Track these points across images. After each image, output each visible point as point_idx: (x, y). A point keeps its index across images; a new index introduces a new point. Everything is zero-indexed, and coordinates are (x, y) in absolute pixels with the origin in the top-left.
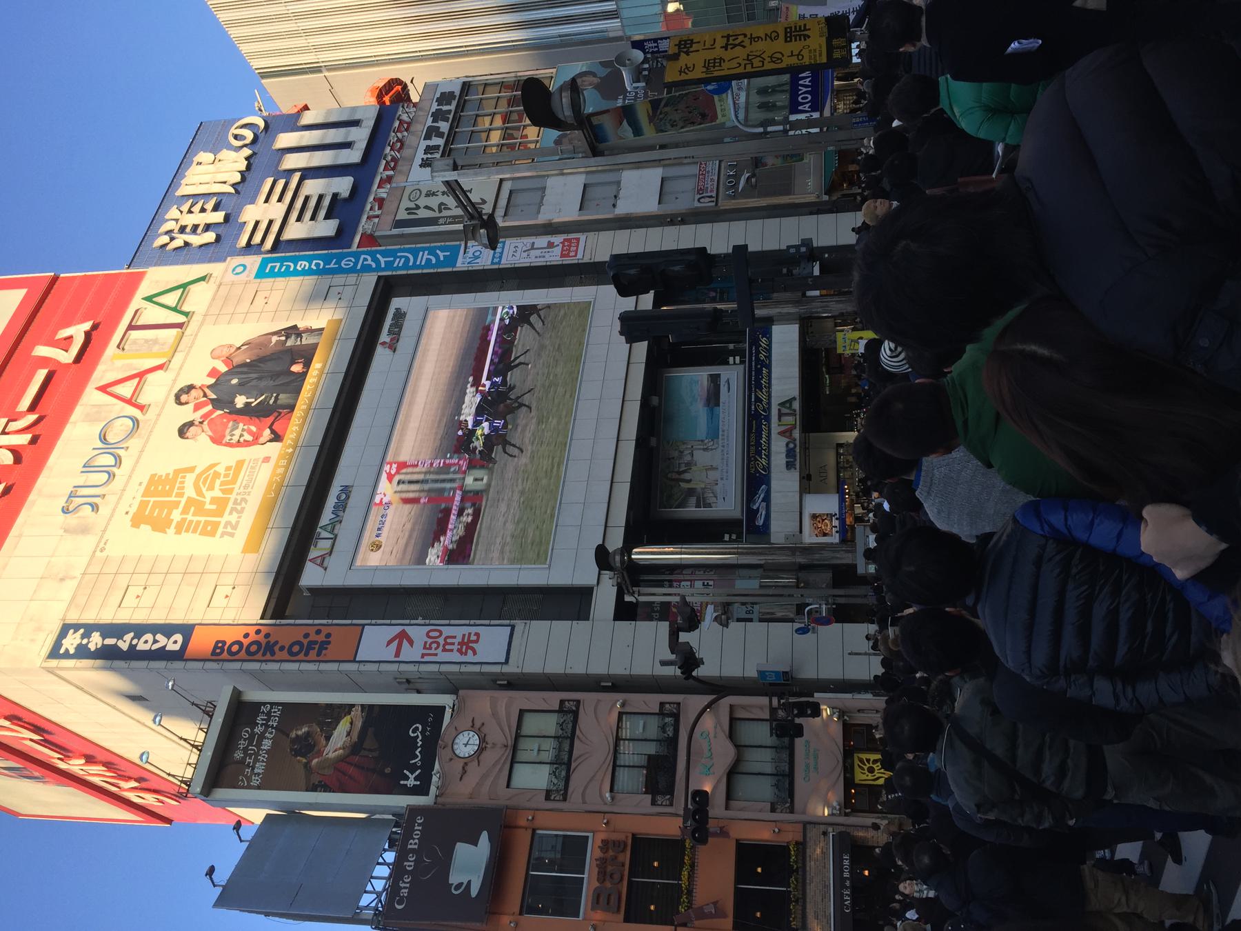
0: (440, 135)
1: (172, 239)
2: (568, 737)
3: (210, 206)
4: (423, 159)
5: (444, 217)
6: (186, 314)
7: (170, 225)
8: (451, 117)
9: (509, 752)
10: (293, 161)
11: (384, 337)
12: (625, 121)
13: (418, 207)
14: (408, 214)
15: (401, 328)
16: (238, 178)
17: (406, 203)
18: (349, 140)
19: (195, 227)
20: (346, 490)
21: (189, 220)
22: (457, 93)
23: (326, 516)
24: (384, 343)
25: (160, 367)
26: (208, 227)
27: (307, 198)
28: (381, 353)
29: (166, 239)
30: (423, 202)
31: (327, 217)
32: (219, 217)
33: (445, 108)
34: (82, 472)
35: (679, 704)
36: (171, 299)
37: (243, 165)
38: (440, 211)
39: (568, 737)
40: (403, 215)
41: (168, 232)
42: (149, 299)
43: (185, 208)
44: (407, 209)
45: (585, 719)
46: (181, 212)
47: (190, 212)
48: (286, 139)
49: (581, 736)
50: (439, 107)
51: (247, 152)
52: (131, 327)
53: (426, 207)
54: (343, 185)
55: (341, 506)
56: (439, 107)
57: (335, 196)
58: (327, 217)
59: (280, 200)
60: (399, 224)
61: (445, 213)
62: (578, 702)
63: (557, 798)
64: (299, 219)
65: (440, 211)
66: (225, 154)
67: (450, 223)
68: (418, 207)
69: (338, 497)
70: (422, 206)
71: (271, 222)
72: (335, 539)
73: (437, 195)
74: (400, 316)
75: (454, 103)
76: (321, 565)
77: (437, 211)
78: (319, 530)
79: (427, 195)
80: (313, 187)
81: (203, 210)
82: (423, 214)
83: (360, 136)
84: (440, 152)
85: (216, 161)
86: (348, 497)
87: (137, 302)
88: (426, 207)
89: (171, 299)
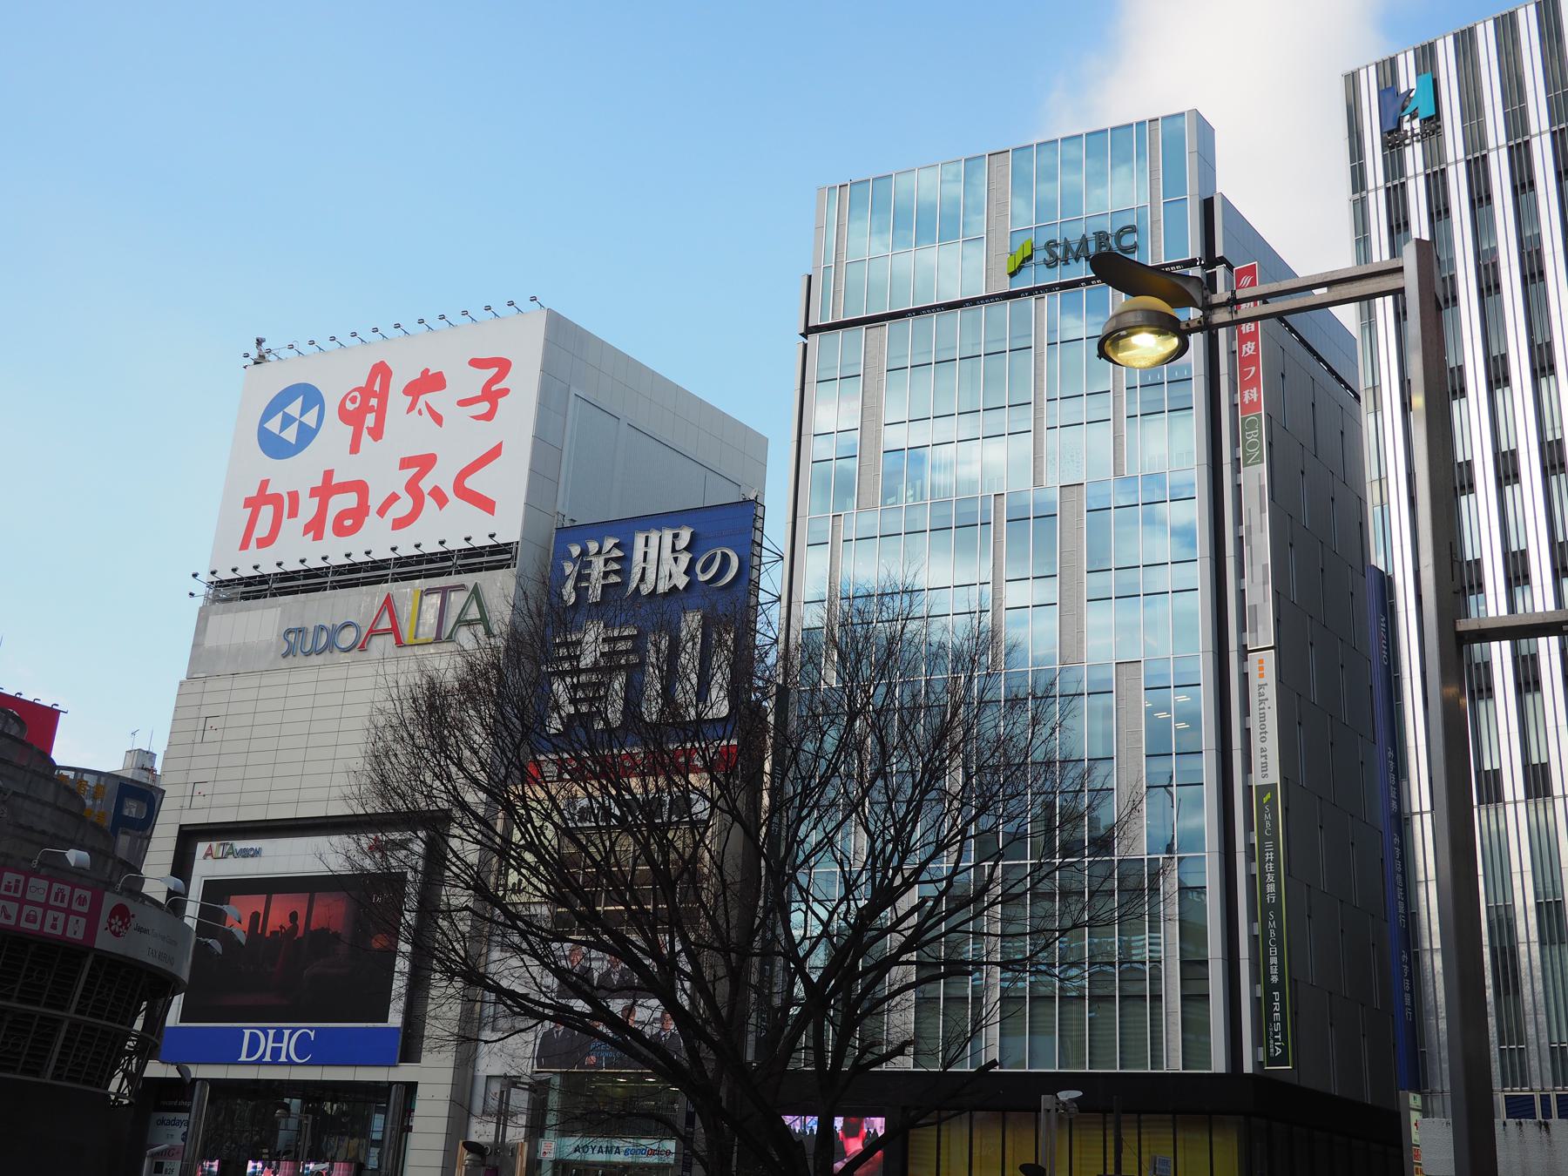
1: (574, 561)
3: (614, 579)
7: (593, 547)
16: (646, 589)
20: (257, 853)
21: (598, 566)
23: (240, 845)
25: (399, 643)
26: (581, 592)
32: (595, 594)
41: (584, 552)
42: (476, 593)
43: (617, 553)
47: (606, 562)
55: (245, 854)
66: (685, 559)
76: (207, 855)
78: (230, 842)
81: (606, 575)
86: (252, 856)
87: (469, 579)
89: (473, 613)
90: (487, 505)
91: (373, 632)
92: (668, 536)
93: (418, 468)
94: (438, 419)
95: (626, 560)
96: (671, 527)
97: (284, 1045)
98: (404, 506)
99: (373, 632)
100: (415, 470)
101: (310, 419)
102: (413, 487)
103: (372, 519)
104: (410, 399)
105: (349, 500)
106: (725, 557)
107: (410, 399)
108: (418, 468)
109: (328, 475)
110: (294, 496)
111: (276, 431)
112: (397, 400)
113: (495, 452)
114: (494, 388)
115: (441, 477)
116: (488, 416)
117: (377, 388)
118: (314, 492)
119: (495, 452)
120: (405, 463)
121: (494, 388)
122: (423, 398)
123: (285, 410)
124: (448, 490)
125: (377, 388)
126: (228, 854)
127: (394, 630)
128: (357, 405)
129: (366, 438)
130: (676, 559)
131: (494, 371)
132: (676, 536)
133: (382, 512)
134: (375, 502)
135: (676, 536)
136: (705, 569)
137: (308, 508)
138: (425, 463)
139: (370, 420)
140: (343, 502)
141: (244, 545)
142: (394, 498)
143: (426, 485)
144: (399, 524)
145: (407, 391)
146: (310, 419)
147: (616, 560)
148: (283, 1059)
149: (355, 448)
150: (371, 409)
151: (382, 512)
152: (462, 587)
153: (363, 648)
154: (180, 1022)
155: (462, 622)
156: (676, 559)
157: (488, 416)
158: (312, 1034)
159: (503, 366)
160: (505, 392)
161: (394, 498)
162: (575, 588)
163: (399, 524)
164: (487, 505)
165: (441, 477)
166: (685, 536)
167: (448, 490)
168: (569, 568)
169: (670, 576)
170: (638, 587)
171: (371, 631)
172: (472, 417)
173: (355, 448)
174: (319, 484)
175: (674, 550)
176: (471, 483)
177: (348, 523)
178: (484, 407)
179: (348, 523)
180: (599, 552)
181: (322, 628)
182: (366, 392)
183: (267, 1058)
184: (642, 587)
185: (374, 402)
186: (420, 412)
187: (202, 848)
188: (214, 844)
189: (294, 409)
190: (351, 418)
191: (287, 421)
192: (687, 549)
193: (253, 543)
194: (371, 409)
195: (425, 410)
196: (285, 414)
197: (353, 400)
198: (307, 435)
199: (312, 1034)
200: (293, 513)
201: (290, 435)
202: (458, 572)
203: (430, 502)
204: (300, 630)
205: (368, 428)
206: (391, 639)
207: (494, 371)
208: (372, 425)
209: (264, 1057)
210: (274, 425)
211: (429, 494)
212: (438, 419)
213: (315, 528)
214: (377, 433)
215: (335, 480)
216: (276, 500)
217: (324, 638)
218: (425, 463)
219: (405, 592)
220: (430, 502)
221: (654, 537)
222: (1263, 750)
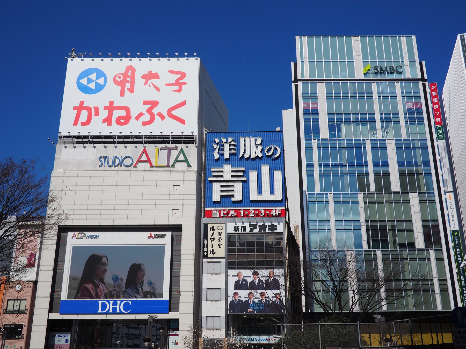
0: (251, 230)
1: (217, 144)
2: (19, 312)
3: (233, 151)
4: (239, 226)
5: (208, 241)
6: (173, 166)
7: (224, 140)
8: (262, 232)
9: (16, 298)
10: (253, 175)
11: (153, 233)
12: (243, 301)
13: (213, 230)
14: (211, 228)
15: (158, 237)
16: (246, 156)
17: (215, 226)
18: (263, 193)
19: (223, 150)
20: (97, 237)
21: (227, 147)
22: (275, 231)
23: (88, 234)
24: (151, 234)
25: (151, 166)
27: (233, 186)
28: (148, 234)
29: (217, 141)
30: (216, 232)
31: (222, 196)
32: (226, 156)
33: (267, 229)
34: (113, 157)
35: (23, 339)
36: (181, 157)
37: (253, 156)
38: (210, 239)
39: (19, 312)
40: (210, 226)
42: (182, 151)
43: (233, 143)
44: (213, 227)
45: (22, 316)
46: (230, 142)
47: (230, 145)
48: (265, 169)
49: (18, 315)
50: (268, 226)
51: (260, 155)
52: (169, 150)
53: (213, 233)
54: (238, 196)
55: (91, 237)
56: (268, 226)
57: (233, 196)
58: (222, 196)
59: (232, 176)
60: (206, 226)
61: (209, 241)
62: (27, 313)
63: (4, 312)
64: (222, 186)
65: (210, 239)
66: (260, 148)
67: (204, 244)
68: (213, 230)
69: (95, 235)
70: (214, 232)
71: (222, 176)
72: (81, 238)
73: (219, 236)
74: (163, 236)
75: (270, 231)
76: (73, 237)
77: (212, 237)
78: (84, 233)
79: (219, 232)
80: (238, 187)
81: (230, 150)
82: (210, 233)
83: (266, 196)
84: (243, 232)
85: (257, 146)
86: (95, 238)
87: (180, 146)
88: (213, 233)
90: (183, 122)
91: (139, 161)
92: (253, 140)
93: (150, 105)
94: (158, 89)
95: (237, 146)
96: (253, 136)
97: (118, 307)
98: (147, 117)
99: (139, 161)
100: (150, 106)
101: (101, 81)
102: (149, 111)
103: (133, 121)
104: (144, 81)
105: (123, 113)
106: (275, 149)
107: (144, 81)
108: (150, 105)
109: (111, 103)
110: (97, 109)
111: (85, 83)
112: (139, 82)
113: (183, 104)
114: (180, 81)
115: (162, 108)
116: (179, 91)
117: (129, 74)
118: (105, 108)
119: (183, 104)
120: (145, 103)
121: (180, 81)
122: (150, 81)
123: (88, 77)
124: (165, 114)
125: (129, 74)
126: (83, 237)
127: (149, 161)
128: (122, 79)
129: (127, 92)
130: (257, 148)
131: (179, 76)
132: (256, 140)
133: (137, 118)
134: (134, 114)
135: (256, 140)
136: (268, 151)
137: (104, 114)
138: (154, 104)
139: (128, 85)
140: (116, 114)
141: (76, 123)
142: (141, 115)
143: (155, 111)
144: (145, 124)
145: (144, 77)
146: (101, 81)
147: (233, 145)
148: (118, 311)
149: (122, 94)
150: (128, 82)
151: (137, 118)
152: (176, 149)
153: (135, 166)
154: (67, 298)
155: (177, 161)
156: (257, 148)
157: (179, 91)
158: (130, 303)
159: (183, 75)
160: (185, 84)
161: (141, 115)
162: (218, 153)
163: (145, 124)
164: (183, 122)
165: (162, 108)
166: (259, 141)
167: (165, 114)
168: (215, 146)
169: (255, 153)
170: (243, 156)
171: (138, 160)
172: (173, 90)
173: (122, 94)
174: (78, 105)
175: (255, 144)
176: (174, 113)
177: (122, 121)
178: (177, 87)
179: (122, 121)
180: (226, 142)
181: (116, 157)
182: (125, 75)
183: (111, 311)
184: (244, 155)
185: (129, 79)
186: (149, 86)
187: (70, 234)
188: (77, 233)
189: (93, 76)
190: (121, 84)
191: (90, 81)
192: (261, 144)
193: (79, 123)
194: (128, 82)
195: (151, 85)
196: (88, 77)
197: (120, 77)
198: (99, 88)
199: (130, 303)
200: (97, 114)
201: (92, 86)
202: (172, 143)
203: (157, 118)
204: (106, 157)
205: (127, 88)
206: (148, 164)
207: (179, 76)
208: (129, 87)
209: (109, 311)
210: (84, 81)
211: (157, 115)
212: (158, 89)
213: (108, 120)
214: (132, 90)
215: (84, 105)
216: (89, 109)
217: (117, 161)
218: (154, 104)
219: (150, 148)
220: (157, 118)
221: (247, 139)
222: (453, 220)
